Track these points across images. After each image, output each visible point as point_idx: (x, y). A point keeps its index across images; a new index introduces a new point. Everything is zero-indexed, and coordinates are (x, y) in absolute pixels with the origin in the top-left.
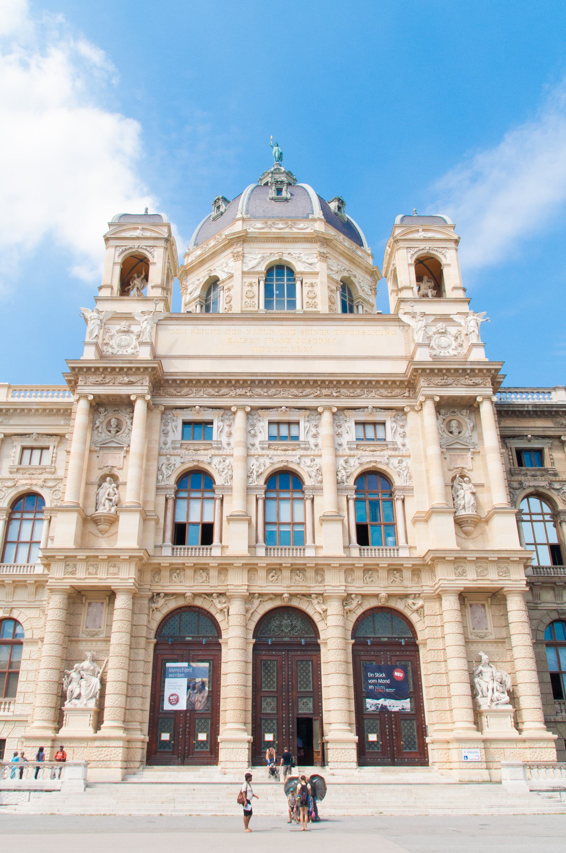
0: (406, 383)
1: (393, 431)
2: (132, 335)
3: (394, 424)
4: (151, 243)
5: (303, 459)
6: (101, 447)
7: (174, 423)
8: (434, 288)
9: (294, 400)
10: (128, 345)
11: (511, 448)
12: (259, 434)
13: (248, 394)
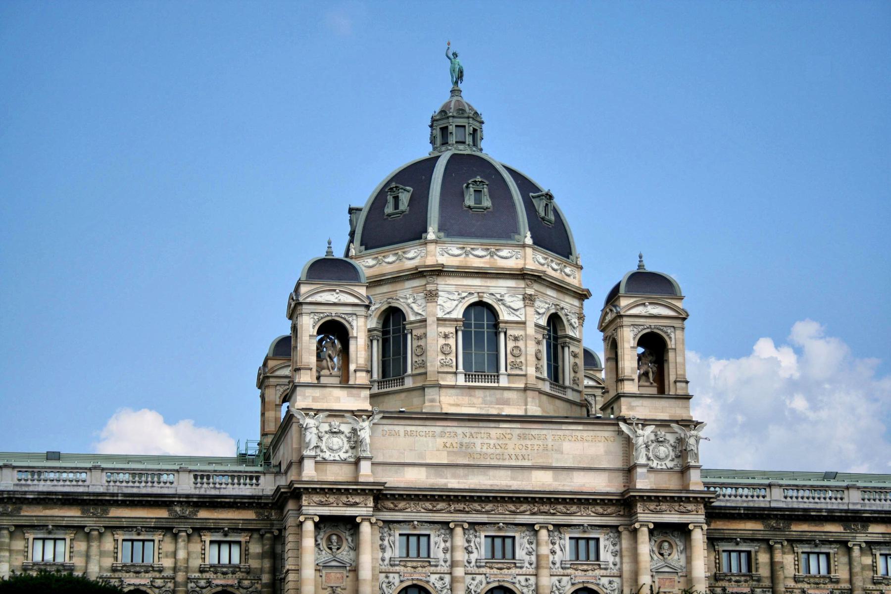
0: (622, 502)
1: (606, 550)
2: (342, 436)
3: (607, 543)
4: (349, 310)
5: (519, 578)
6: (323, 566)
7: (392, 538)
8: (655, 362)
9: (511, 516)
10: (340, 449)
11: (718, 551)
12: (475, 550)
13: (467, 509)
